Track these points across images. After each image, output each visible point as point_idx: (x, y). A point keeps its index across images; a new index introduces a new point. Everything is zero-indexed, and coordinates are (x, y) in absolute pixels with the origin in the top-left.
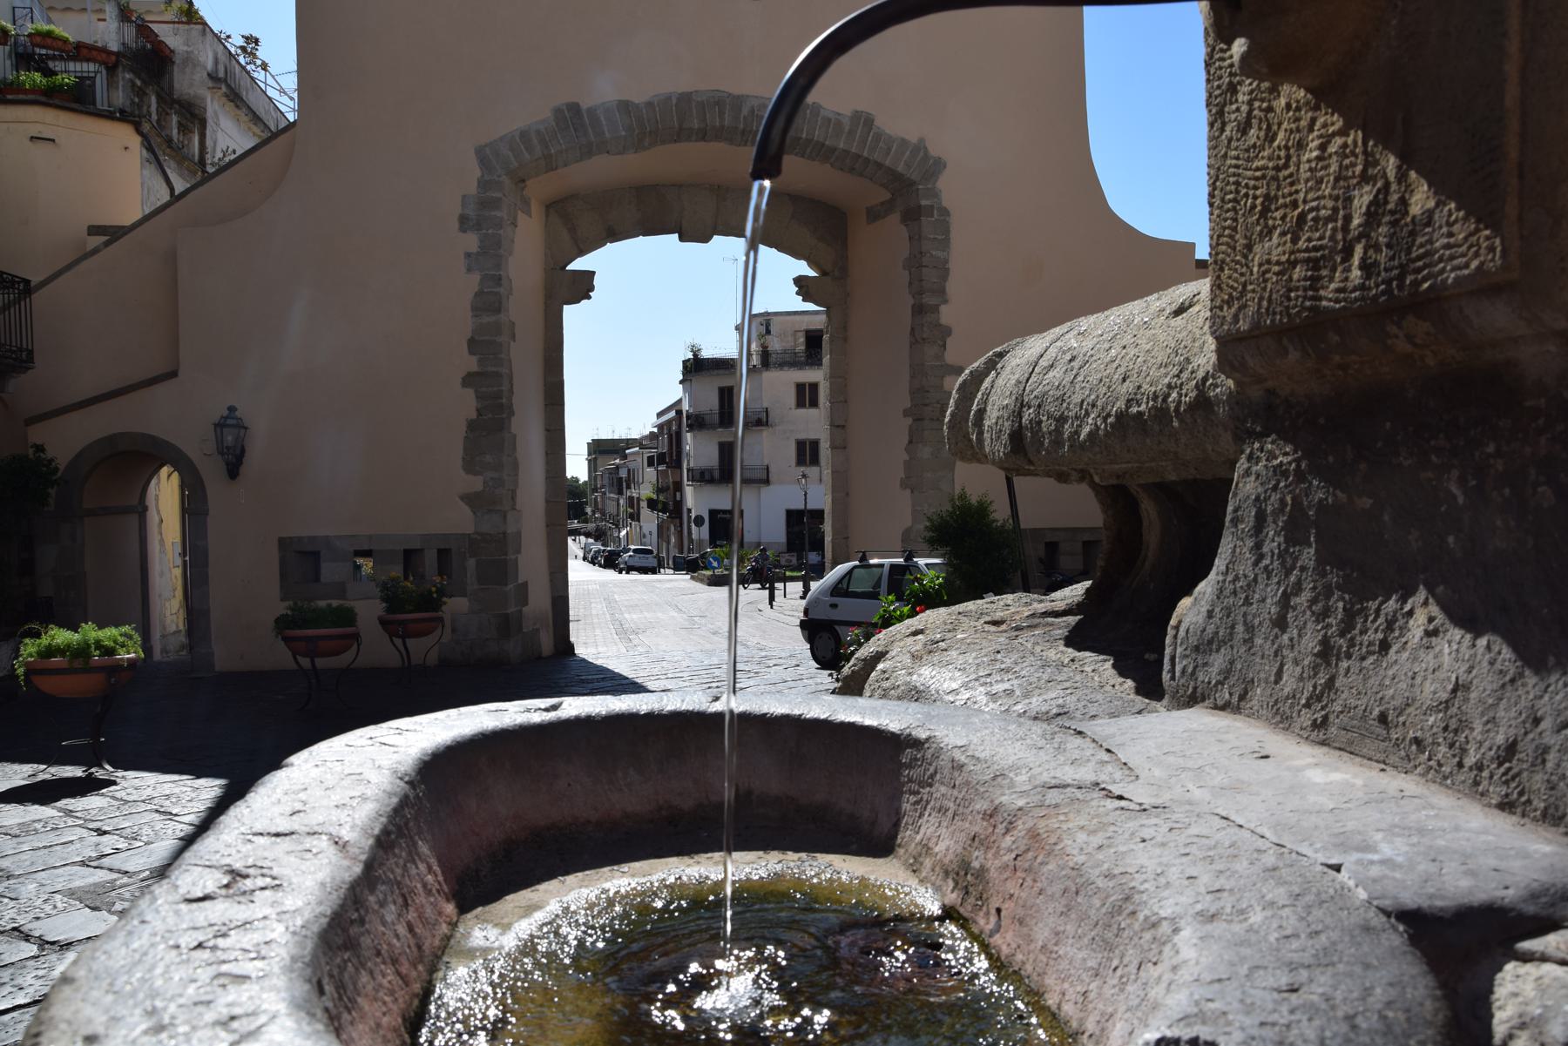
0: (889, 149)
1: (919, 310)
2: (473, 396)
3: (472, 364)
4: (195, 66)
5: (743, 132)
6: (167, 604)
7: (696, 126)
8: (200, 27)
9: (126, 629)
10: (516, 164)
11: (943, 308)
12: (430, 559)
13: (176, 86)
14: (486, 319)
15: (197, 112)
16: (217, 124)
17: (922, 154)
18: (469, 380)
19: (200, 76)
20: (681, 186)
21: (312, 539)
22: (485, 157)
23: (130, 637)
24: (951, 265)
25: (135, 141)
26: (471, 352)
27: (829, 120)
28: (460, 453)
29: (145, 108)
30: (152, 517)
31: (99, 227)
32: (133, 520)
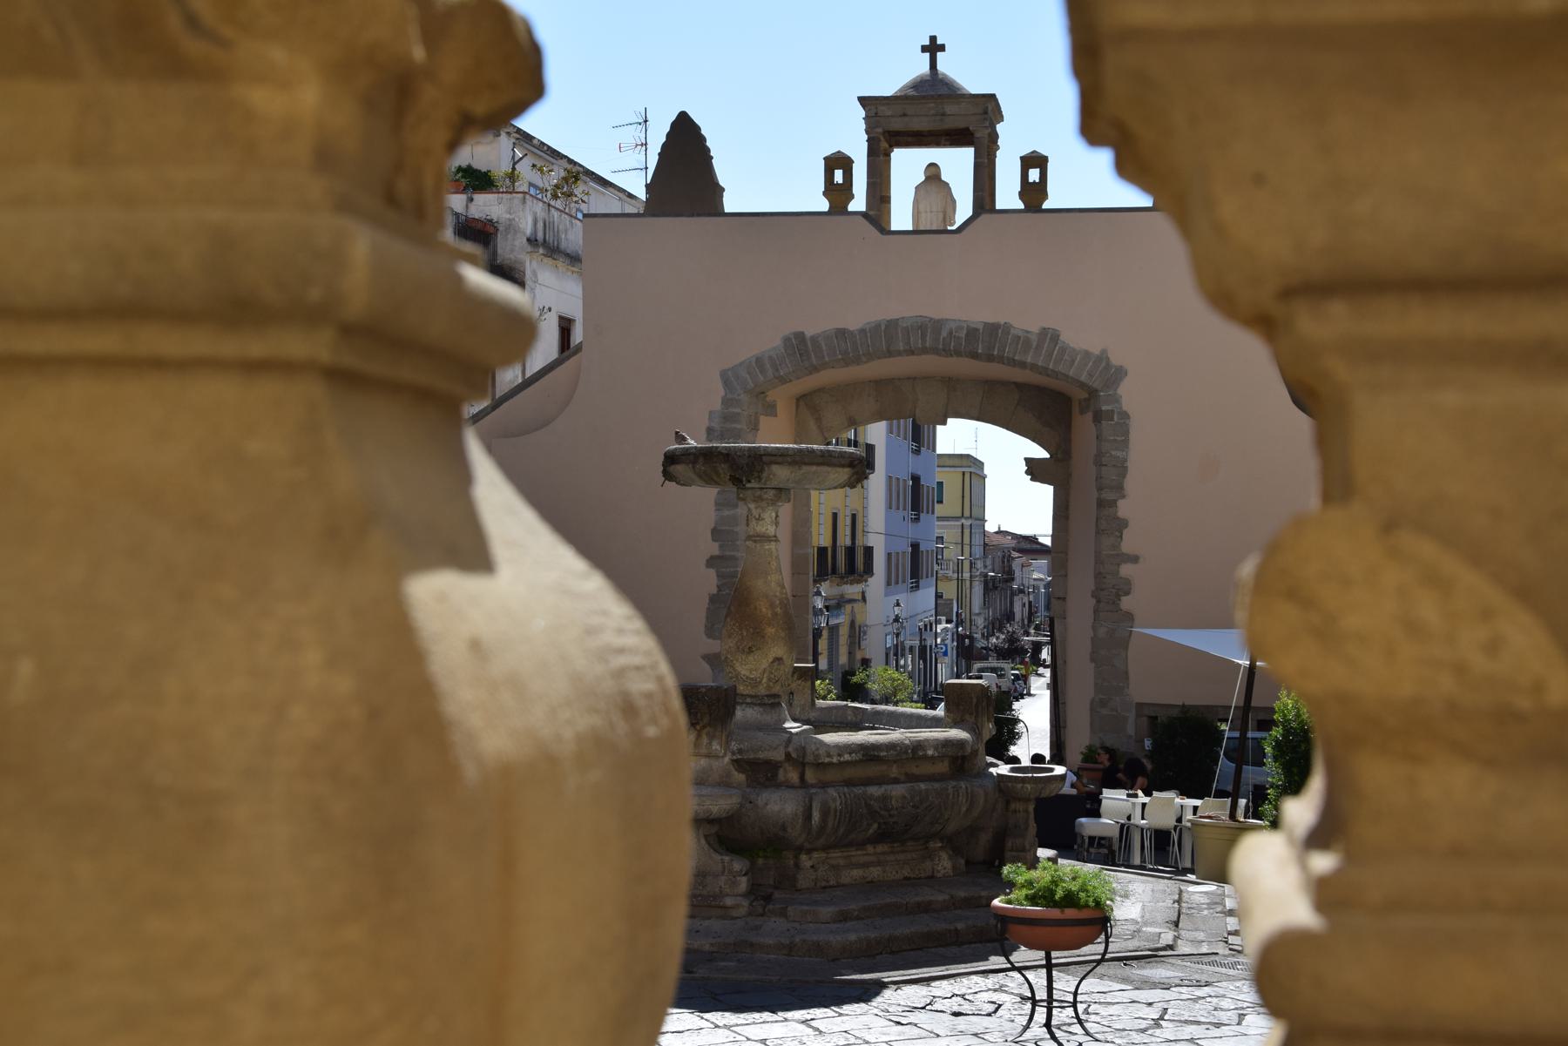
0: (1073, 361)
1: (1101, 504)
2: (715, 574)
3: (714, 549)
4: (516, 232)
5: (944, 350)
7: (902, 348)
8: (521, 196)
10: (752, 385)
11: (1121, 503)
13: (499, 251)
14: (726, 513)
15: (517, 276)
17: (1103, 364)
18: (712, 562)
19: (521, 241)
20: (915, 378)
22: (727, 379)
24: (1129, 464)
27: (1019, 337)
28: (704, 620)
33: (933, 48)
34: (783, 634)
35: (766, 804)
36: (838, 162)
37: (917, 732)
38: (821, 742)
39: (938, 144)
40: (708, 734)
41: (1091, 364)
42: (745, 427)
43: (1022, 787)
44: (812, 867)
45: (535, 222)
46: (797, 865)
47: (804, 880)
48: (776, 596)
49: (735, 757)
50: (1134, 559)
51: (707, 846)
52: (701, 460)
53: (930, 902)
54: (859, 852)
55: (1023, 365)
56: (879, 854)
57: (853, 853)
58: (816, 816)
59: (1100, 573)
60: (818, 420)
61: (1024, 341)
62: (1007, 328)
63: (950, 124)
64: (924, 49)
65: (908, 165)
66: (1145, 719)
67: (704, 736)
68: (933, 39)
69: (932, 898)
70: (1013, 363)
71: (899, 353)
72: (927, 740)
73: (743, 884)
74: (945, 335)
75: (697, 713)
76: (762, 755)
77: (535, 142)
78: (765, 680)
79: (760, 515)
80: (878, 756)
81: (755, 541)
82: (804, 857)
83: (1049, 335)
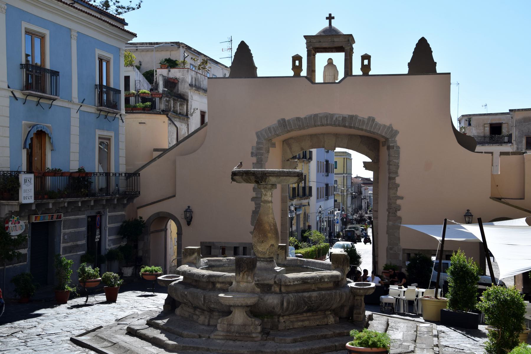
0: (380, 128)
1: (390, 178)
4: (185, 82)
5: (334, 124)
6: (172, 257)
7: (319, 124)
8: (187, 69)
9: (159, 267)
11: (397, 178)
12: (241, 250)
13: (179, 89)
15: (186, 97)
16: (192, 99)
17: (390, 129)
18: (253, 199)
19: (187, 85)
20: (324, 134)
21: (209, 243)
22: (258, 135)
23: (160, 269)
24: (399, 164)
25: (167, 119)
26: (254, 191)
27: (361, 120)
28: (250, 220)
29: (170, 105)
30: (169, 231)
31: (156, 149)
32: (163, 233)
33: (330, 18)
34: (274, 236)
35: (267, 300)
36: (297, 58)
37: (321, 273)
38: (287, 277)
39: (332, 52)
40: (246, 275)
41: (386, 129)
42: (264, 152)
43: (359, 291)
44: (284, 322)
45: (192, 78)
46: (278, 321)
47: (281, 326)
48: (271, 222)
49: (256, 283)
50: (402, 198)
51: (246, 315)
52: (245, 175)
53: (326, 335)
54: (301, 316)
55: (362, 130)
56: (308, 316)
57: (299, 316)
58: (285, 304)
59: (390, 203)
60: (291, 149)
61: (362, 121)
62: (356, 117)
63: (336, 45)
64: (327, 18)
65: (321, 59)
66: (406, 254)
67: (245, 275)
68: (330, 15)
69: (327, 333)
70: (358, 129)
71: (318, 126)
72: (325, 276)
73: (259, 329)
74: (334, 120)
75: (243, 267)
76: (266, 282)
77: (192, 49)
78: (268, 252)
79: (266, 194)
80: (307, 282)
81: (264, 203)
82: (281, 318)
83: (371, 119)
